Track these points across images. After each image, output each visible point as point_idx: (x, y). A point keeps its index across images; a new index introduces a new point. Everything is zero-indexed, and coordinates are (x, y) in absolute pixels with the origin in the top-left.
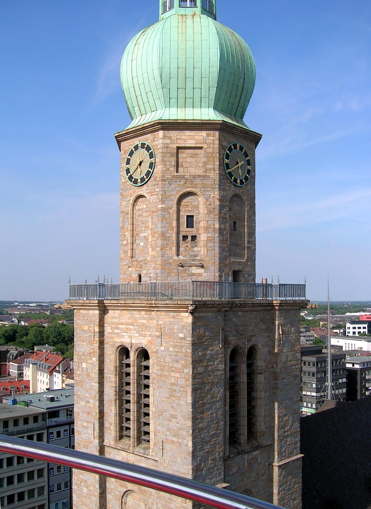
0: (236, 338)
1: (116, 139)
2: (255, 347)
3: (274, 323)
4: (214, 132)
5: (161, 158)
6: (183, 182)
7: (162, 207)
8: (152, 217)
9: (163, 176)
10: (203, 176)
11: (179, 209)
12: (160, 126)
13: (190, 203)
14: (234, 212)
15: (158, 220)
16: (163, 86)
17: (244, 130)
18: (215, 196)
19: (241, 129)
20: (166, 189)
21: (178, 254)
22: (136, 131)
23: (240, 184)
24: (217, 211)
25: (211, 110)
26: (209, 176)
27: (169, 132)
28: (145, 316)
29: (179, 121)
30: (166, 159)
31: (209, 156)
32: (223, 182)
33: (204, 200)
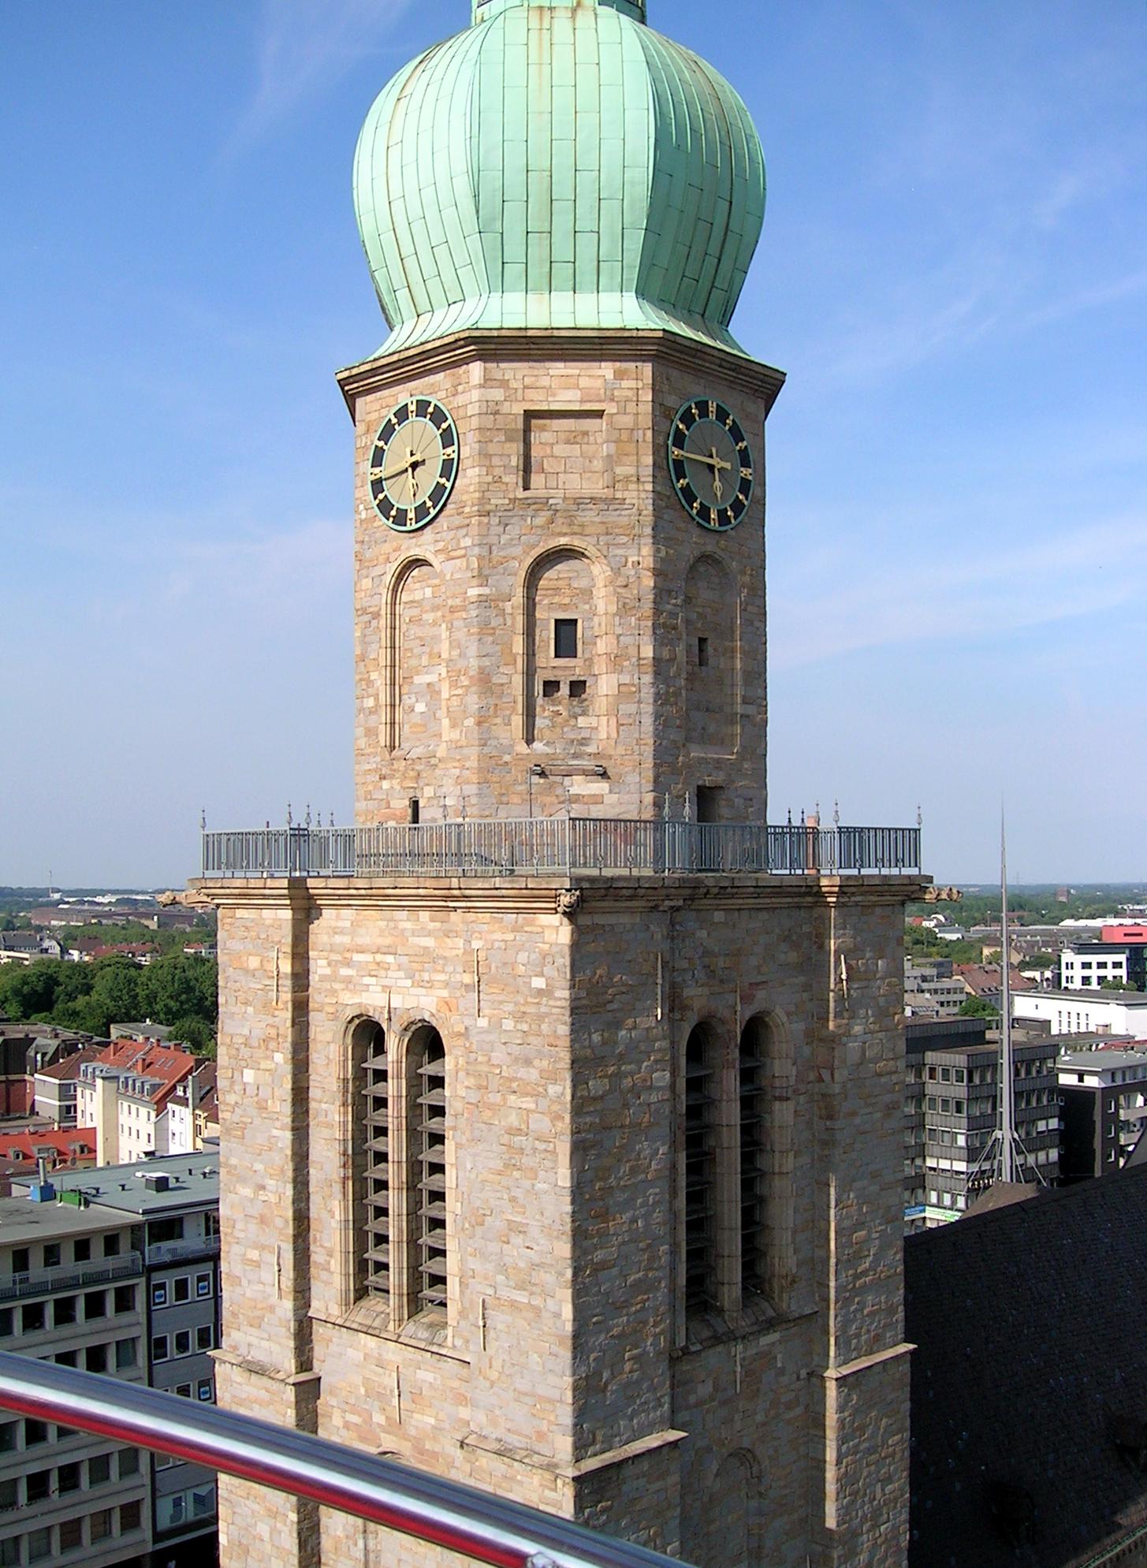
0: (706, 991)
1: (343, 389)
2: (767, 1019)
3: (822, 947)
4: (638, 364)
5: (477, 446)
6: (544, 519)
7: (480, 595)
8: (449, 625)
9: (483, 500)
10: (604, 500)
11: (534, 599)
12: (472, 347)
13: (566, 582)
14: (700, 610)
15: (470, 634)
16: (484, 226)
17: (729, 358)
18: (641, 559)
19: (722, 356)
20: (494, 539)
21: (530, 737)
22: (401, 364)
23: (717, 525)
24: (647, 607)
25: (630, 297)
26: (625, 499)
27: (500, 365)
28: (432, 925)
29: (530, 333)
30: (492, 448)
31: (624, 437)
32: (666, 517)
33: (607, 574)
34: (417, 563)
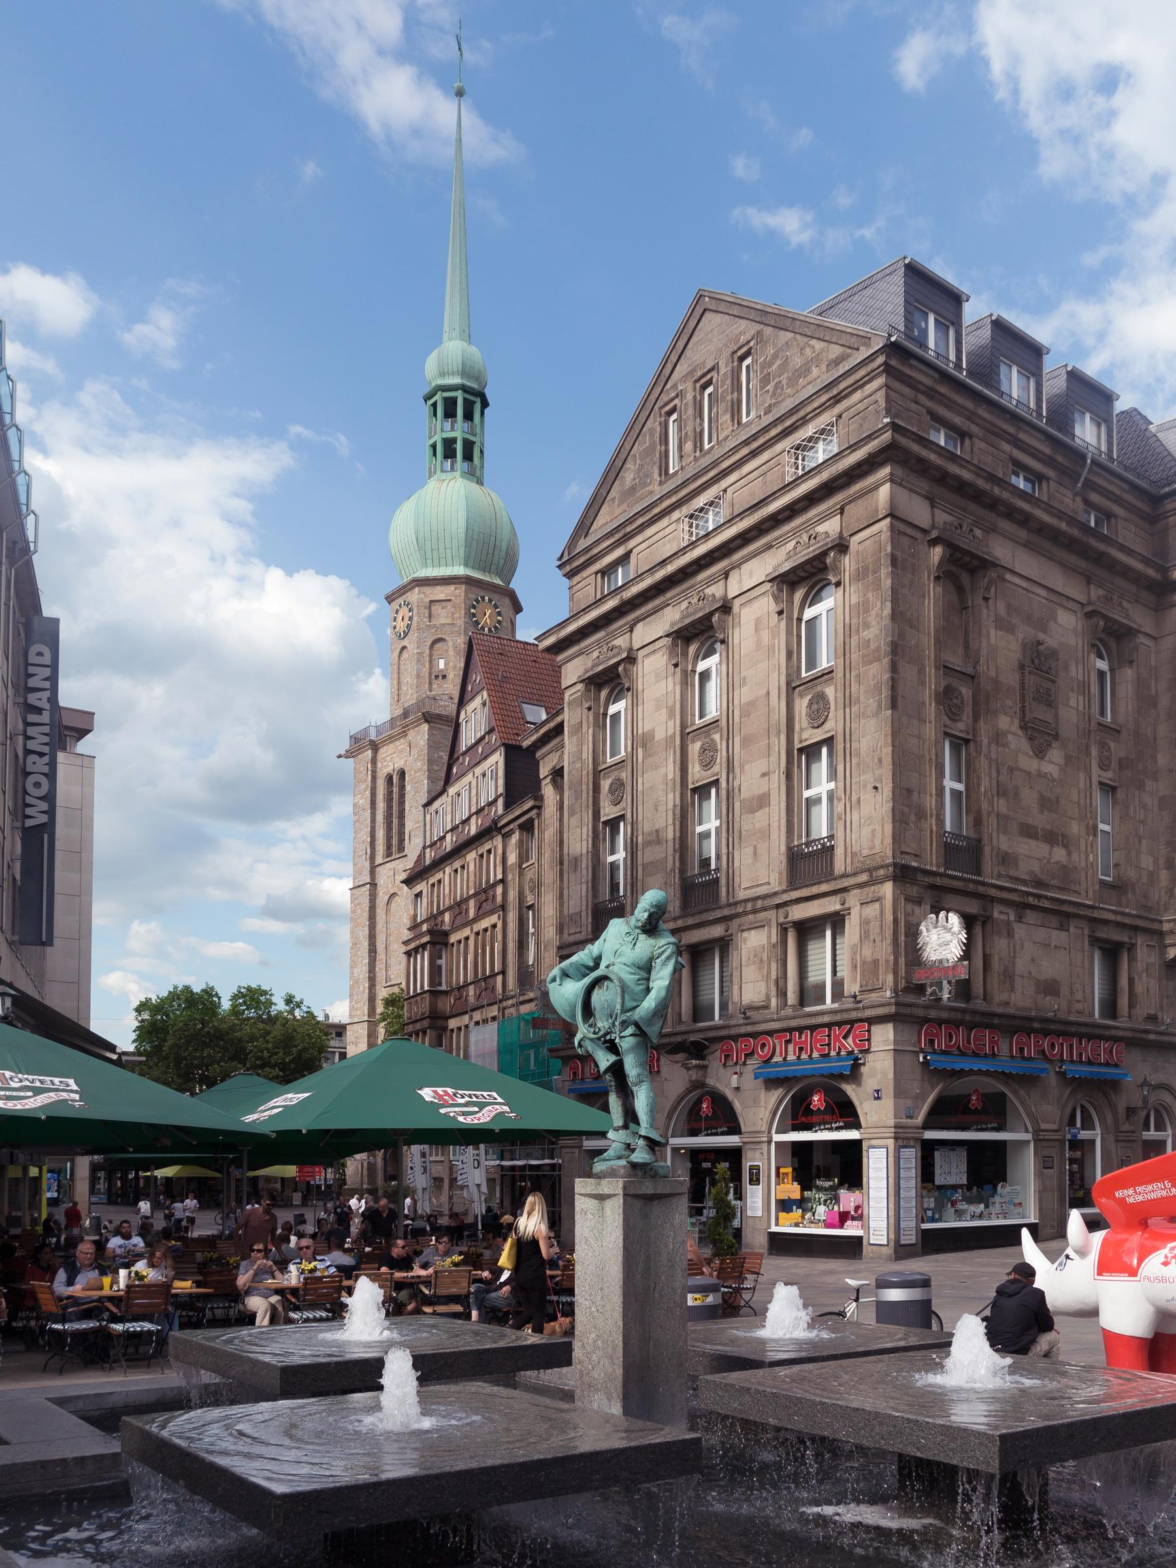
34: (404, 648)
